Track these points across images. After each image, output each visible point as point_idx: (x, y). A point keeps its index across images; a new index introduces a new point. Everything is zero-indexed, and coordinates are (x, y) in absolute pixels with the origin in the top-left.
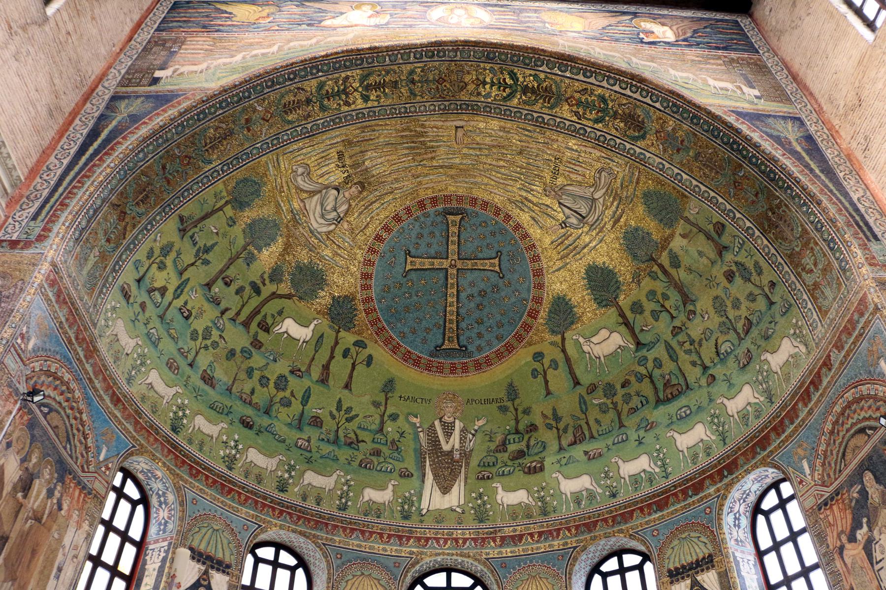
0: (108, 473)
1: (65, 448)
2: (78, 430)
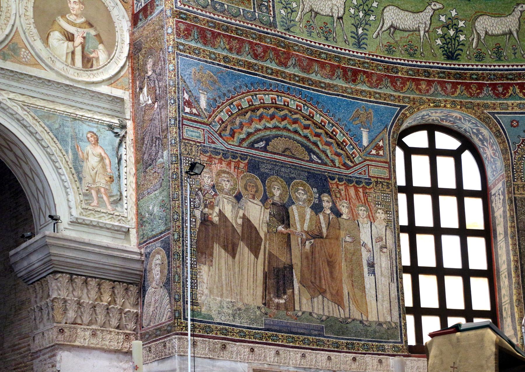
0: (381, 153)
1: (311, 161)
2: (318, 135)
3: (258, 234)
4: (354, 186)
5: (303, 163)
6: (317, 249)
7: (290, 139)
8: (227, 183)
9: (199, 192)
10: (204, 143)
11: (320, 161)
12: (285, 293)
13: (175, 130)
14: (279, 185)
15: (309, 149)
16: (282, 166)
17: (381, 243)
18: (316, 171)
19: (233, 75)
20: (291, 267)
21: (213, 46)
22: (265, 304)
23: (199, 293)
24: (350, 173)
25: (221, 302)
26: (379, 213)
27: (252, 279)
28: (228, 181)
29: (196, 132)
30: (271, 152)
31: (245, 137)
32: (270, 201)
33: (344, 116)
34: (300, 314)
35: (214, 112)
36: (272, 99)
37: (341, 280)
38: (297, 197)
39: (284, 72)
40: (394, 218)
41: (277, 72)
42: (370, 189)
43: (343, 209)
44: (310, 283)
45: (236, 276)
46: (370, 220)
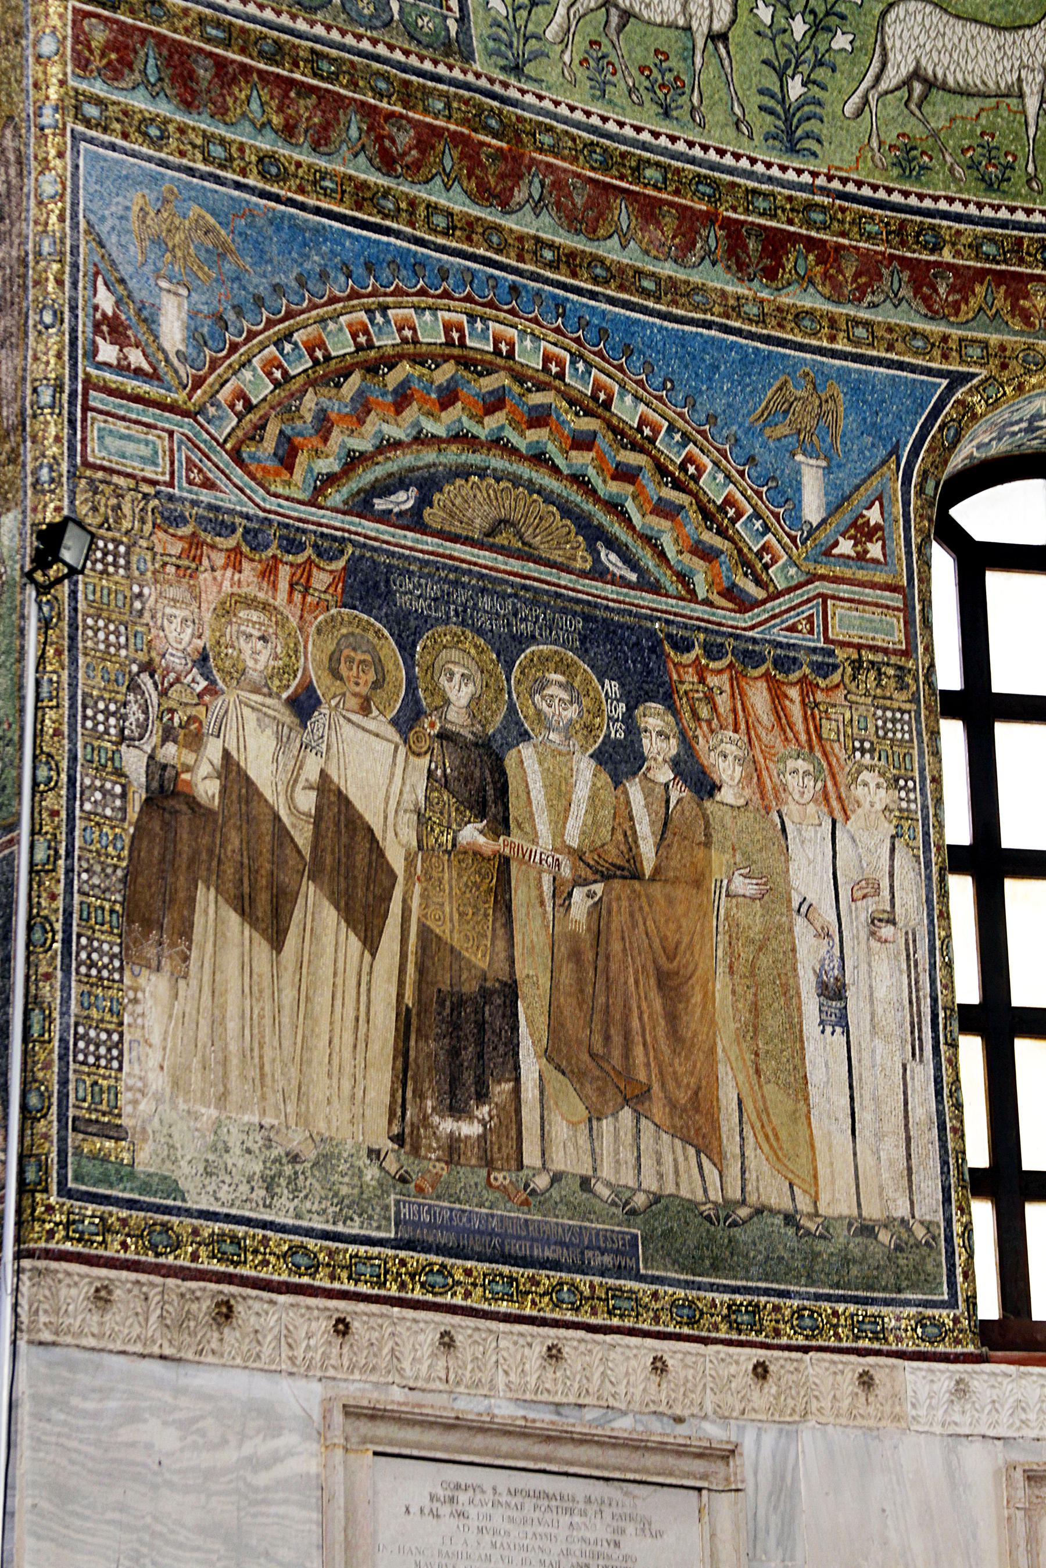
0: (875, 550)
1: (599, 573)
3: (381, 854)
4: (766, 675)
5: (565, 579)
6: (614, 926)
7: (516, 486)
8: (260, 644)
9: (145, 677)
10: (172, 486)
11: (633, 577)
12: (482, 1096)
13: (52, 430)
14: (467, 661)
15: (589, 525)
16: (483, 590)
17: (871, 905)
18: (619, 612)
19: (296, 227)
20: (510, 991)
21: (220, 113)
22: (399, 1139)
23: (129, 1089)
24: (752, 628)
25: (218, 1124)
26: (866, 784)
27: (348, 1037)
28: (263, 638)
29: (138, 441)
31: (336, 468)
32: (432, 725)
33: (730, 405)
34: (542, 1182)
35: (214, 365)
36: (448, 328)
37: (712, 1050)
38: (539, 712)
39: (498, 228)
40: (925, 807)
41: (470, 224)
42: (828, 689)
43: (721, 764)
44: (585, 1057)
45: (286, 1020)
46: (831, 813)
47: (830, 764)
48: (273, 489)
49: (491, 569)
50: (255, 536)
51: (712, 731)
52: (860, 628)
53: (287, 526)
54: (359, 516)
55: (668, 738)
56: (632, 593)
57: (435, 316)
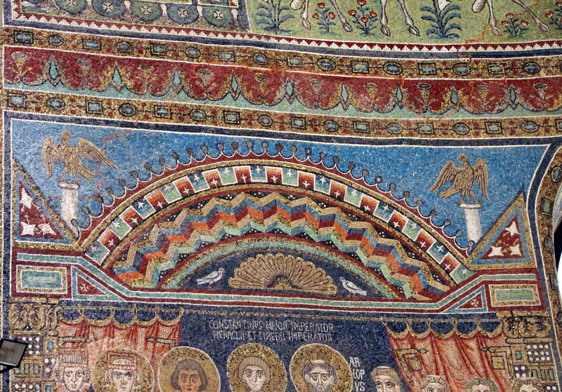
4: (454, 337)
5: (320, 302)
7: (286, 254)
8: (126, 378)
10: (69, 296)
14: (260, 362)
16: (268, 319)
18: (357, 315)
24: (442, 309)
28: (128, 374)
29: (48, 275)
30: (240, 291)
31: (172, 266)
33: (417, 184)
35: (95, 223)
36: (239, 175)
38: (308, 384)
39: (267, 115)
41: (250, 116)
42: (494, 338)
47: (500, 384)
48: (133, 285)
49: (273, 305)
50: (123, 315)
51: (422, 376)
52: (511, 297)
53: (142, 305)
54: (187, 291)
55: (393, 385)
56: (364, 302)
57: (231, 170)
